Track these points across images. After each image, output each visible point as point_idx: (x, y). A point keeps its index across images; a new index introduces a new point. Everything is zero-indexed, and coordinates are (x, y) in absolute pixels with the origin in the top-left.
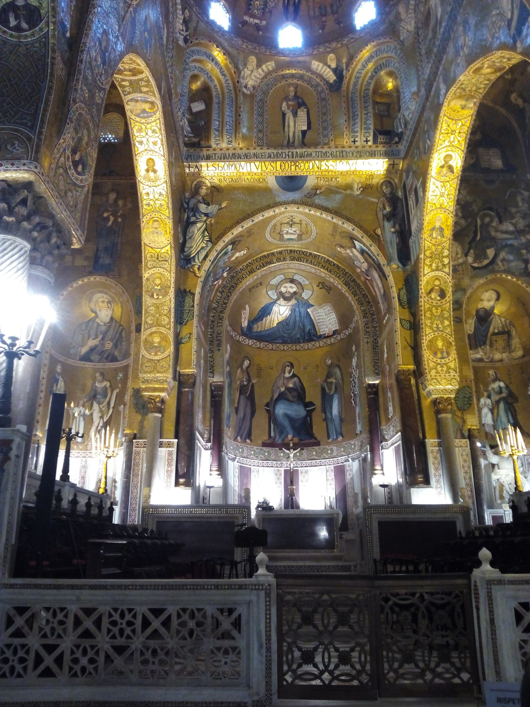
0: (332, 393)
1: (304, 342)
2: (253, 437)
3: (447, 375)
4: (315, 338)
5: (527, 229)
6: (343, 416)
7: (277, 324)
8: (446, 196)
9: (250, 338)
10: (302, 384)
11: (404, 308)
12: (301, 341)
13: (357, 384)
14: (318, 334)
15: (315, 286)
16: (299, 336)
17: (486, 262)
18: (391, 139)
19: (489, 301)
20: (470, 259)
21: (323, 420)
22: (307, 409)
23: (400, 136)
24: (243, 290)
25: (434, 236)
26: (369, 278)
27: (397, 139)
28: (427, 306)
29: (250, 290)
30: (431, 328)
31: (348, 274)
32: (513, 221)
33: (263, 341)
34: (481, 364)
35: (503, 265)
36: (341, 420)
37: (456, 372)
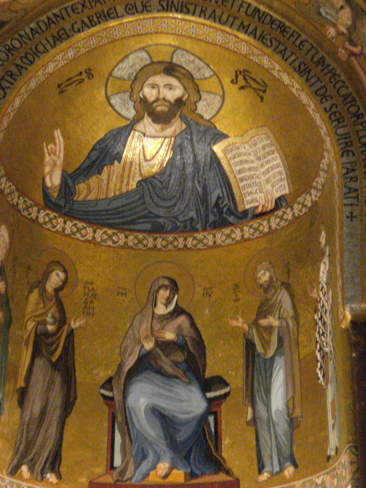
0: (271, 353)
1: (204, 229)
2: (63, 469)
4: (231, 219)
6: (297, 413)
7: (139, 183)
9: (70, 215)
10: (197, 331)
12: (199, 226)
13: (329, 328)
14: (240, 209)
15: (226, 81)
16: (193, 214)
21: (248, 424)
22: (210, 395)
24: (41, 86)
26: (356, 50)
29: (61, 89)
31: (307, 46)
33: (102, 225)
36: (293, 423)
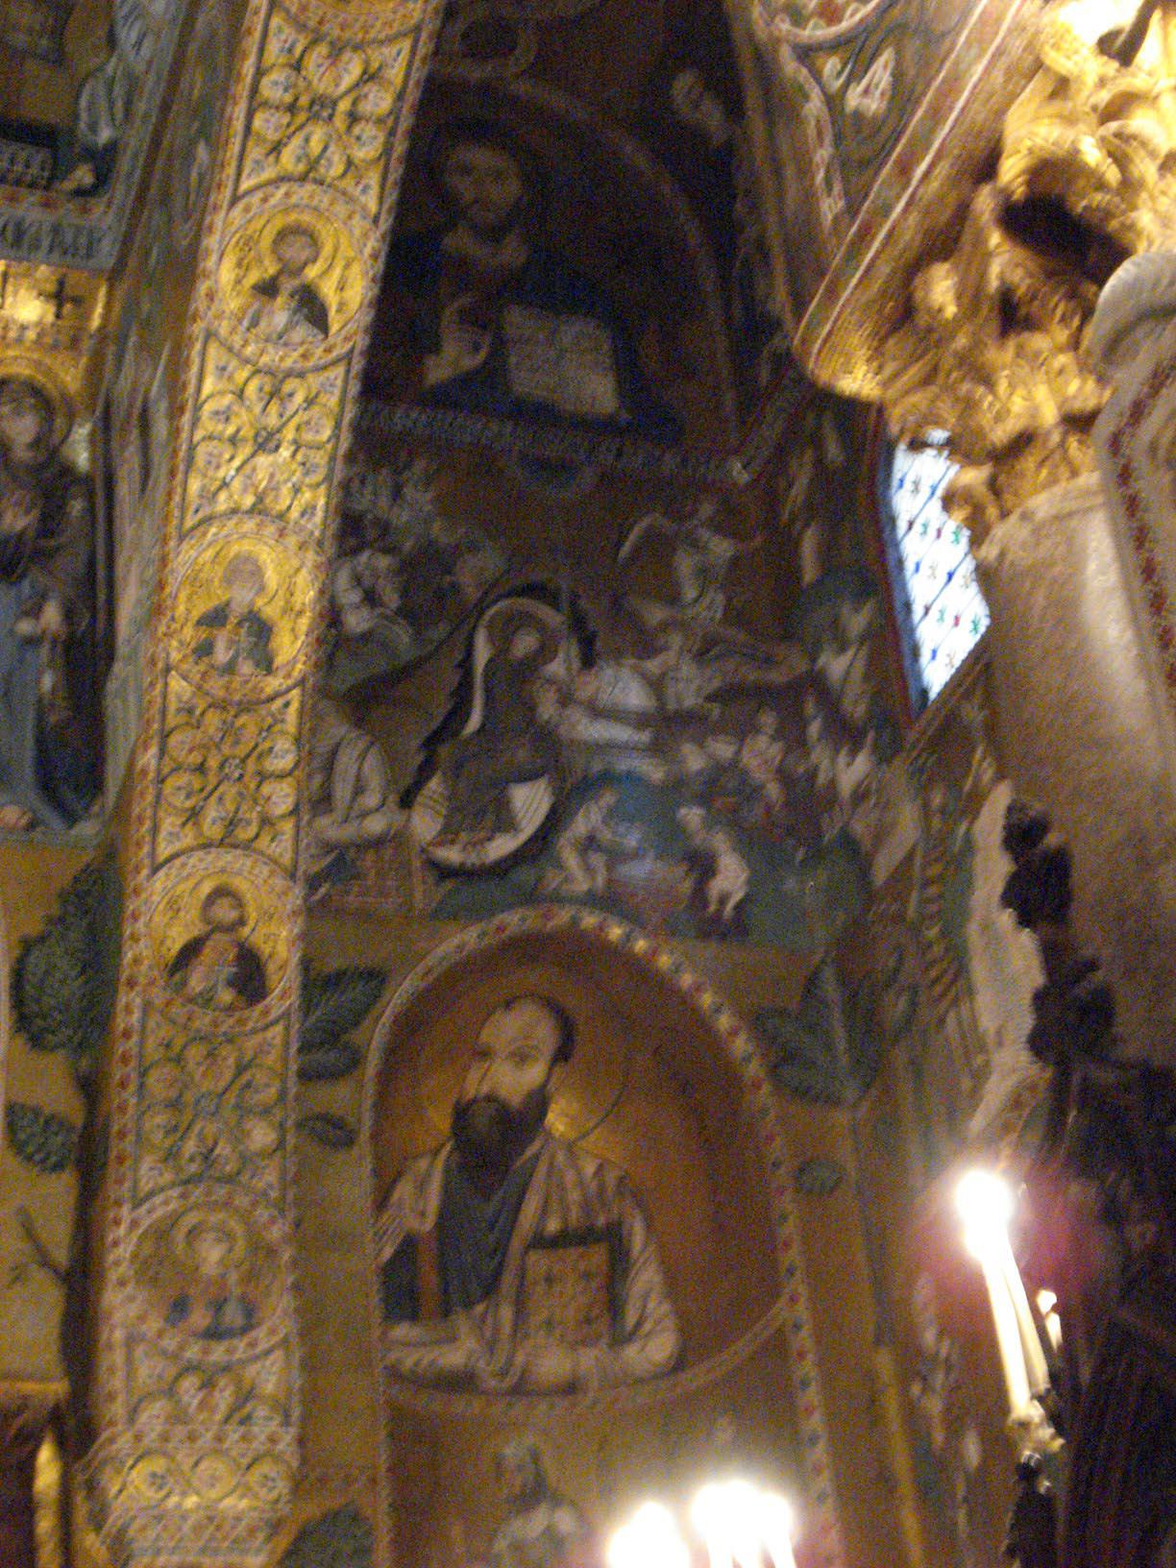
3: (234, 1434)
5: (715, 710)
8: (285, 452)
11: (37, 1042)
17: (502, 846)
18: (57, 171)
19: (521, 1058)
20: (424, 824)
23: (104, 161)
25: (222, 655)
27: (84, 175)
28: (159, 1031)
30: (171, 1156)
32: (653, 666)
34: (460, 1405)
35: (589, 869)
37: (286, 1422)
